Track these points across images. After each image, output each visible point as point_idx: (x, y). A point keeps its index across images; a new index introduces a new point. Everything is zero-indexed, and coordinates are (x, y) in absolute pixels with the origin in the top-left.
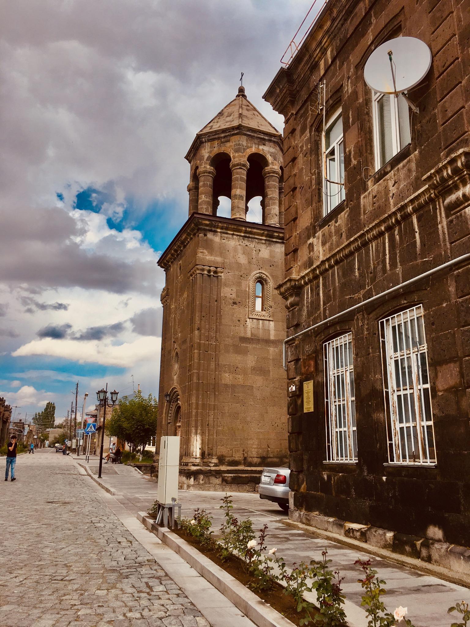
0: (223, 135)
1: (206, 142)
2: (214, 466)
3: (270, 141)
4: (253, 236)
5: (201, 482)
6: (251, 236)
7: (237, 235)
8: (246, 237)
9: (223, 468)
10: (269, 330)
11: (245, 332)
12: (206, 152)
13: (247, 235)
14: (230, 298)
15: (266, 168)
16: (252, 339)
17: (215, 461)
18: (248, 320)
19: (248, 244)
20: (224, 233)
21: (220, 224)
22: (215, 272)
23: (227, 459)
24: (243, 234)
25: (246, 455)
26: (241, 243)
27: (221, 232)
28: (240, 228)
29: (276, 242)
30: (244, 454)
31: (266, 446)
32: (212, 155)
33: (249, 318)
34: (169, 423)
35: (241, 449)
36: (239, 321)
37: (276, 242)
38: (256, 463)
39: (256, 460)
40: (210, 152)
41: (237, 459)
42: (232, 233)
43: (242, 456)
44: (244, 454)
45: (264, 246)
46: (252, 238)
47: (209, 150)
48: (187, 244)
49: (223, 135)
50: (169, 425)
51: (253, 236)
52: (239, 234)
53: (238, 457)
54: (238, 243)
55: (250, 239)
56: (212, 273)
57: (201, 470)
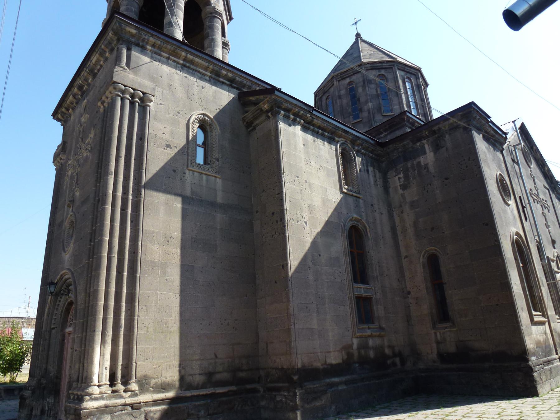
2: (130, 397)
4: (195, 68)
6: (192, 66)
7: (174, 61)
8: (185, 66)
10: (215, 190)
13: (188, 65)
18: (187, 172)
20: (156, 53)
21: (151, 39)
22: (141, 99)
23: (153, 382)
24: (181, 62)
27: (151, 51)
29: (223, 83)
31: (213, 356)
33: (189, 170)
34: (54, 328)
36: (174, 171)
38: (198, 384)
42: (167, 55)
46: (193, 70)
48: (99, 70)
50: (53, 331)
51: (195, 68)
52: (176, 60)
55: (191, 71)
57: (107, 406)
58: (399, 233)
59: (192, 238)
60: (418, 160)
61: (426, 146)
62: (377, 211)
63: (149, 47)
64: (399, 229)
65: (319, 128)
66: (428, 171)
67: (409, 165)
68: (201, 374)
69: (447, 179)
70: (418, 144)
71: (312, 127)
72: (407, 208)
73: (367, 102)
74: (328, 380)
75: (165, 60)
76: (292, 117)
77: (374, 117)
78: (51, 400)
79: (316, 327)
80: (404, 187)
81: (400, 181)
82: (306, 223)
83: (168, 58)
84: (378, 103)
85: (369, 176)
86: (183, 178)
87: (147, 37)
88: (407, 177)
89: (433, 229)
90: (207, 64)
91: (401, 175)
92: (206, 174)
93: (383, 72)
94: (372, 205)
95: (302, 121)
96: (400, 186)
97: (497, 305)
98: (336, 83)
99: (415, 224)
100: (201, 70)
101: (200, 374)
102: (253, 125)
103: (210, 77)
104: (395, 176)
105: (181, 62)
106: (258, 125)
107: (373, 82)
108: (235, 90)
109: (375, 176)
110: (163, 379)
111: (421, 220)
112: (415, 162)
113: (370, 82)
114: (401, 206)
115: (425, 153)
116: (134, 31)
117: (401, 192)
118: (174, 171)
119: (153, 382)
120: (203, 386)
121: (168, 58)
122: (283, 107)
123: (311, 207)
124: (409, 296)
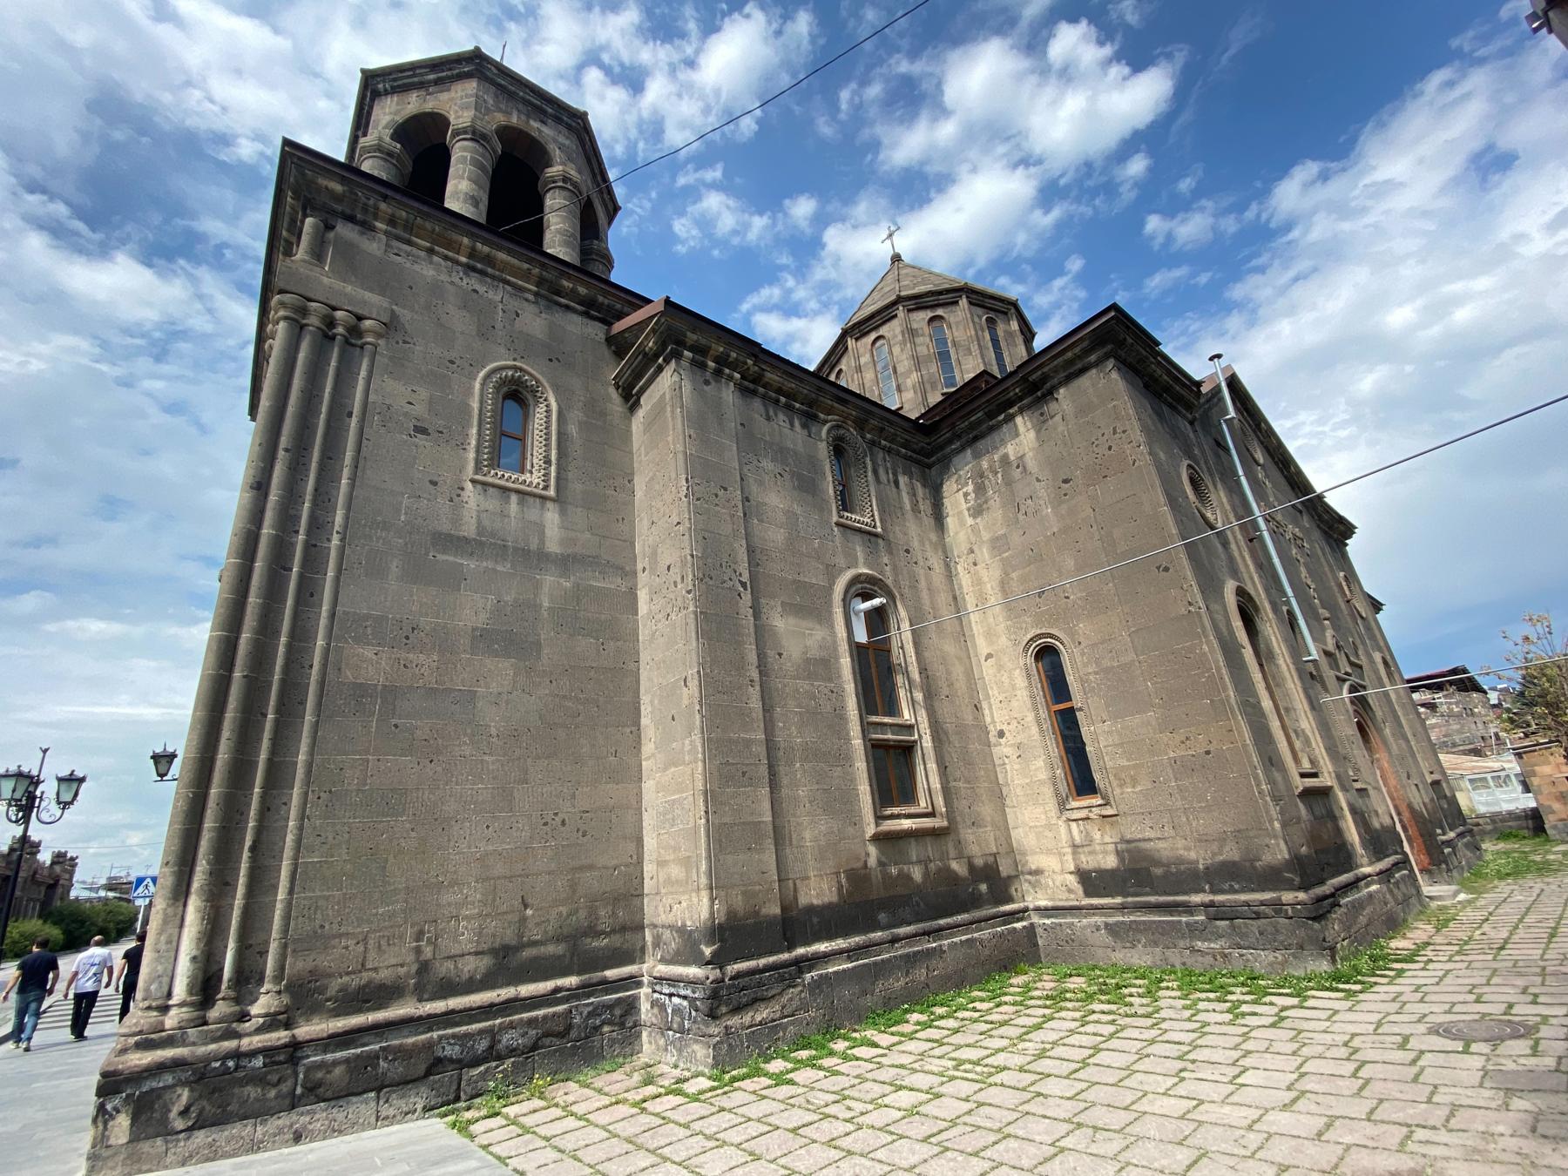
0: (432, 77)
1: (386, 93)
3: (558, 120)
6: (490, 270)
7: (446, 258)
8: (474, 269)
11: (457, 520)
12: (388, 113)
14: (406, 414)
16: (481, 544)
19: (481, 289)
20: (398, 238)
21: (383, 206)
23: (334, 986)
24: (463, 259)
25: (428, 952)
26: (457, 280)
27: (386, 233)
28: (456, 237)
29: (567, 307)
30: (418, 951)
31: (517, 903)
32: (399, 119)
36: (434, 483)
37: (567, 307)
39: (473, 966)
41: (384, 975)
43: (411, 958)
45: (532, 308)
47: (394, 107)
49: (432, 77)
53: (391, 963)
54: (444, 277)
56: (340, 330)
59: (474, 630)
60: (1002, 451)
62: (921, 563)
65: (779, 391)
67: (985, 464)
68: (482, 953)
69: (1066, 481)
71: (761, 390)
72: (984, 554)
75: (423, 254)
76: (711, 364)
80: (977, 512)
81: (966, 501)
82: (744, 585)
83: (431, 251)
86: (456, 499)
87: (371, 202)
88: (980, 489)
90: (526, 266)
91: (970, 488)
92: (518, 492)
93: (940, 312)
94: (907, 551)
95: (737, 376)
97: (1208, 753)
98: (850, 342)
99: (1004, 585)
101: (477, 953)
105: (463, 259)
109: (913, 494)
111: (1014, 575)
112: (996, 457)
115: (1017, 435)
116: (337, 187)
117: (970, 521)
118: (434, 483)
120: (487, 983)
121: (431, 251)
122: (689, 342)
124: (1003, 741)
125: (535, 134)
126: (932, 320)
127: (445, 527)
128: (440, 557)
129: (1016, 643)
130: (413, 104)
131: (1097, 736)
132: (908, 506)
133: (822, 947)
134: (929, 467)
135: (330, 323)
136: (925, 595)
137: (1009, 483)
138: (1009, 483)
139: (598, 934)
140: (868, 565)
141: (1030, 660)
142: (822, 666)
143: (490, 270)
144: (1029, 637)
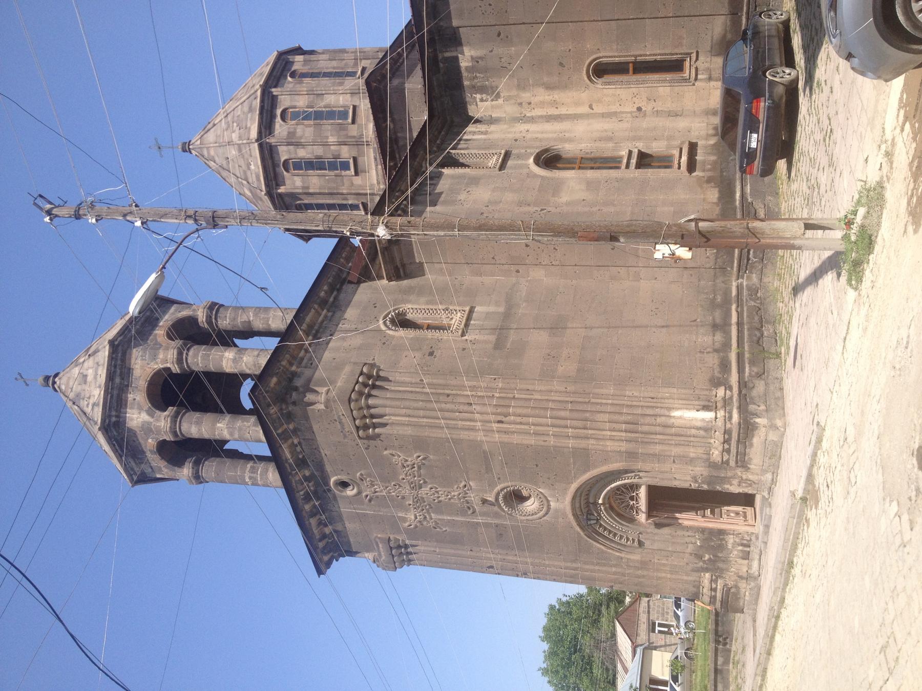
5: (763, 407)
6: (316, 328)
9: (734, 378)
10: (488, 313)
13: (314, 332)
15: (200, 320)
17: (721, 392)
21: (284, 363)
29: (335, 298)
30: (709, 352)
32: (147, 405)
35: (699, 355)
40: (140, 409)
41: (717, 362)
44: (709, 352)
46: (320, 327)
47: (135, 411)
53: (713, 360)
57: (739, 408)
58: (556, 112)
60: (463, 70)
61: (447, 54)
63: (294, 368)
64: (552, 111)
66: (481, 58)
69: (499, 35)
70: (441, 65)
72: (526, 96)
73: (325, 145)
74: (738, 203)
77: (354, 137)
78: (731, 540)
79: (672, 209)
82: (542, 210)
84: (329, 127)
85: (474, 140)
89: (561, 64)
91: (478, 96)
96: (492, 100)
99: (549, 87)
100: (321, 319)
102: (399, 266)
103: (328, 311)
104: (477, 105)
106: (401, 260)
107: (292, 130)
108: (344, 287)
109: (474, 133)
110: (715, 366)
113: (291, 134)
114: (520, 104)
116: (274, 380)
117: (500, 101)
119: (717, 374)
120: (728, 335)
123: (520, 204)
124: (644, 109)
125: (170, 323)
126: (283, 118)
127: (491, 346)
128: (508, 346)
129: (587, 87)
130: (137, 396)
131: (651, 51)
132: (483, 137)
133: (738, 195)
134: (452, 122)
135: (365, 385)
136: (545, 136)
137: (485, 70)
138: (485, 70)
139: (714, 298)
140: (529, 158)
141: (600, 81)
142: (591, 185)
143: (316, 328)
144: (586, 78)
